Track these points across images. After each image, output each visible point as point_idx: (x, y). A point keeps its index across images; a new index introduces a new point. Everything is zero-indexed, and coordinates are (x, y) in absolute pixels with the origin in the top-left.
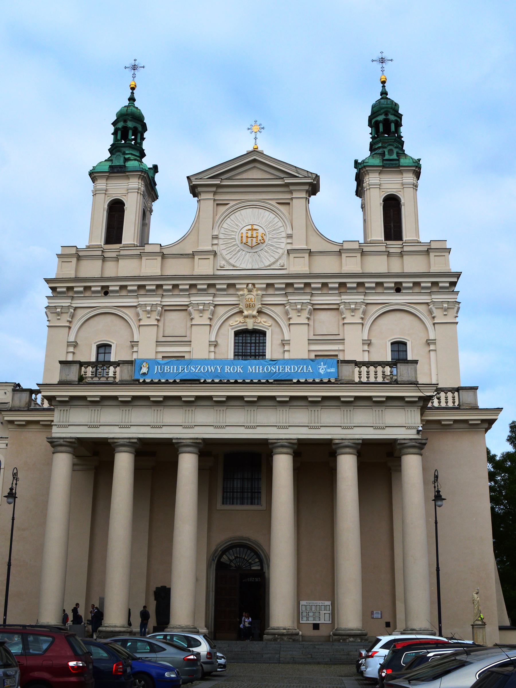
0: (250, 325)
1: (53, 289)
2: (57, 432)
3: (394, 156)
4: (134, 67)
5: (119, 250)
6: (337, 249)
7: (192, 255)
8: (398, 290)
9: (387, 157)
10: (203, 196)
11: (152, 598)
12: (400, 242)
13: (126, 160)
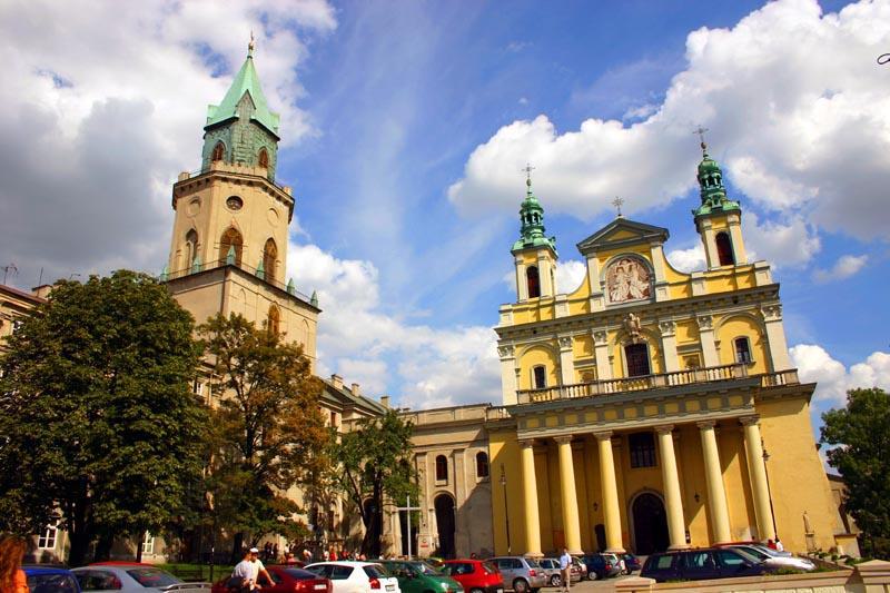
0: (635, 341)
1: (500, 335)
2: (522, 435)
3: (719, 205)
4: (528, 169)
5: (538, 302)
6: (685, 279)
7: (588, 299)
8: (736, 302)
9: (714, 206)
10: (589, 255)
11: (594, 532)
12: (732, 266)
13: (534, 237)
